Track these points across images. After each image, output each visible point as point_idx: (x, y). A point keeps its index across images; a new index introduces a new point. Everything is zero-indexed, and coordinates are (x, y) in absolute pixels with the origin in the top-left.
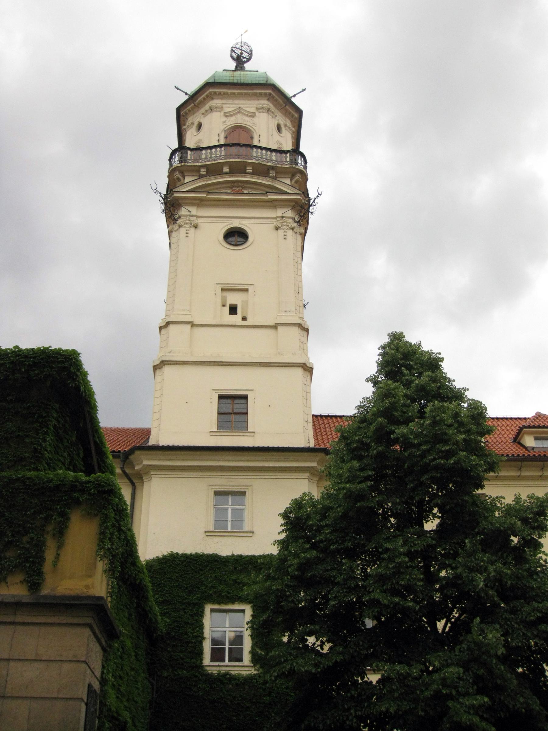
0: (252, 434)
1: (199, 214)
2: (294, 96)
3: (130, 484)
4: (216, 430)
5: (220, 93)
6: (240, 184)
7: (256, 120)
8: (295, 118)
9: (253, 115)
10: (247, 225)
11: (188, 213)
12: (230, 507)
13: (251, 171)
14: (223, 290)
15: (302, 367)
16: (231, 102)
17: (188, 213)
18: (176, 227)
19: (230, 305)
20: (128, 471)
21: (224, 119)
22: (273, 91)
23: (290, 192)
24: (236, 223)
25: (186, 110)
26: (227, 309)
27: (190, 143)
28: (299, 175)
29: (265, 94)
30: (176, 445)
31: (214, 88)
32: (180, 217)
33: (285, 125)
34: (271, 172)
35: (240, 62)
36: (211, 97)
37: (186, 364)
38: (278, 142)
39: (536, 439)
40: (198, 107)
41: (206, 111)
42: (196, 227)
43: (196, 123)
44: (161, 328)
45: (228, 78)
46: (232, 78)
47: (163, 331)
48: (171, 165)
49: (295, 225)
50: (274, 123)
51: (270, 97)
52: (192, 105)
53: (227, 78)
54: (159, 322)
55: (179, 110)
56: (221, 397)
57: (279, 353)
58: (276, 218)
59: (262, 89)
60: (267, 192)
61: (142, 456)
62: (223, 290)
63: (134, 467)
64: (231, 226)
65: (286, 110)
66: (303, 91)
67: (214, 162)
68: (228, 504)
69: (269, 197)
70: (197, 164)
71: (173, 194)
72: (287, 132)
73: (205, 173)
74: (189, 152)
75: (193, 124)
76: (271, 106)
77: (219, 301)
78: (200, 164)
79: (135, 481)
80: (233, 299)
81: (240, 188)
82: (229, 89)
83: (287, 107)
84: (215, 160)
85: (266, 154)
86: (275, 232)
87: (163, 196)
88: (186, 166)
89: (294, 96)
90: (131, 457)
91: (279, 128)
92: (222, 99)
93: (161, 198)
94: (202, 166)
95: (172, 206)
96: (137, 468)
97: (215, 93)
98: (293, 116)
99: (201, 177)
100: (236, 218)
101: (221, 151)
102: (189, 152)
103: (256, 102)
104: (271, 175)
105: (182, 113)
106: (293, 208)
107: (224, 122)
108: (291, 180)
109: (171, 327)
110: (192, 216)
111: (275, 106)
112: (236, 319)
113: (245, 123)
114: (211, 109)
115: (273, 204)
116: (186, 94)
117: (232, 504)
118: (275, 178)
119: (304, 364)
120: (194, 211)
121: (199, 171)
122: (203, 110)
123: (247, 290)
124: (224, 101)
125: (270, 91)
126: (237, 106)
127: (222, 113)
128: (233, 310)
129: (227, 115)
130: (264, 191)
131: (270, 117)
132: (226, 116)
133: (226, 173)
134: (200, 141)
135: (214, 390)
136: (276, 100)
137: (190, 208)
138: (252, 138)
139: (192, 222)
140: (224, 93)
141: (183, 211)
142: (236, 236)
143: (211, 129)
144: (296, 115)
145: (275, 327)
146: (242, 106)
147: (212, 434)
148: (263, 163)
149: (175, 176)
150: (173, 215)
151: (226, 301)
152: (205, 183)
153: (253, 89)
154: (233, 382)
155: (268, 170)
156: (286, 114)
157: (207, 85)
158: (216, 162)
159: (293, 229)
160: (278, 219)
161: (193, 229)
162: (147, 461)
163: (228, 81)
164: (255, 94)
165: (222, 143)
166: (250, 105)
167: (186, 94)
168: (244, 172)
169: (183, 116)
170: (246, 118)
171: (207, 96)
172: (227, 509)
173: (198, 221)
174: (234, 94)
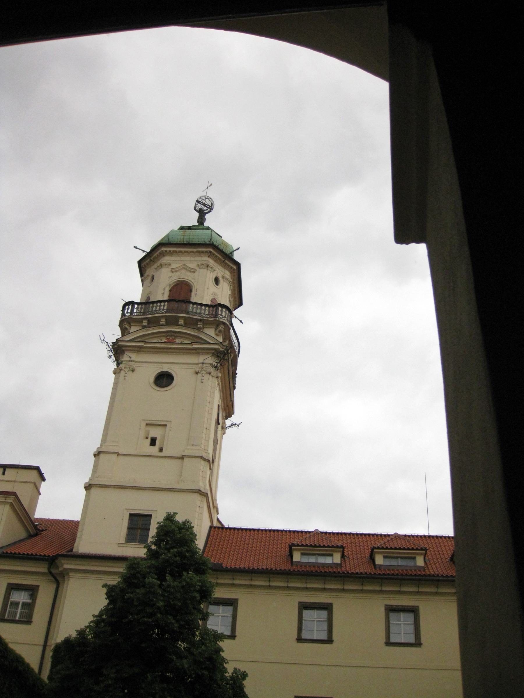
1: (136, 360)
4: (123, 542)
5: (170, 251)
6: (173, 334)
7: (196, 275)
8: (234, 269)
9: (193, 271)
10: (175, 370)
11: (128, 359)
14: (147, 425)
15: (198, 493)
16: (179, 259)
20: (53, 571)
21: (170, 274)
22: (214, 249)
23: (211, 342)
24: (166, 368)
26: (149, 441)
28: (222, 326)
29: (206, 252)
33: (223, 277)
34: (199, 323)
35: (202, 215)
36: (163, 254)
37: (109, 487)
38: (214, 294)
39: (385, 557)
40: (153, 261)
41: (158, 266)
42: (133, 371)
43: (151, 276)
45: (179, 237)
46: (182, 237)
48: (123, 314)
49: (212, 370)
50: (211, 276)
51: (210, 255)
55: (140, 263)
56: (131, 515)
58: (198, 364)
59: (204, 248)
61: (63, 561)
62: (147, 425)
65: (226, 263)
72: (225, 283)
73: (146, 324)
75: (148, 276)
76: (211, 262)
77: (142, 434)
79: (59, 579)
81: (173, 337)
83: (226, 261)
84: (155, 314)
85: (197, 308)
86: (195, 375)
88: (132, 318)
90: (56, 561)
91: (217, 281)
92: (172, 256)
93: (107, 347)
94: (144, 319)
96: (60, 569)
97: (166, 251)
98: (232, 268)
99: (144, 327)
103: (199, 259)
104: (198, 326)
105: (142, 265)
106: (213, 354)
107: (171, 277)
108: (216, 330)
110: (132, 361)
111: (215, 261)
112: (154, 450)
114: (161, 266)
115: (197, 352)
116: (144, 251)
118: (199, 329)
119: (199, 490)
120: (134, 356)
121: (142, 322)
122: (155, 266)
124: (173, 258)
125: (211, 250)
126: (183, 263)
127: (170, 270)
128: (153, 442)
129: (172, 271)
131: (209, 271)
132: (173, 272)
133: (163, 325)
135: (126, 509)
136: (216, 256)
137: (130, 354)
140: (174, 251)
142: (164, 379)
144: (235, 267)
145: (182, 458)
146: (185, 263)
147: (120, 545)
149: (125, 323)
151: (148, 434)
156: (226, 267)
157: (160, 245)
159: (210, 373)
161: (131, 372)
162: (67, 565)
164: (199, 252)
166: (192, 261)
170: (189, 274)
171: (160, 253)
173: (136, 366)
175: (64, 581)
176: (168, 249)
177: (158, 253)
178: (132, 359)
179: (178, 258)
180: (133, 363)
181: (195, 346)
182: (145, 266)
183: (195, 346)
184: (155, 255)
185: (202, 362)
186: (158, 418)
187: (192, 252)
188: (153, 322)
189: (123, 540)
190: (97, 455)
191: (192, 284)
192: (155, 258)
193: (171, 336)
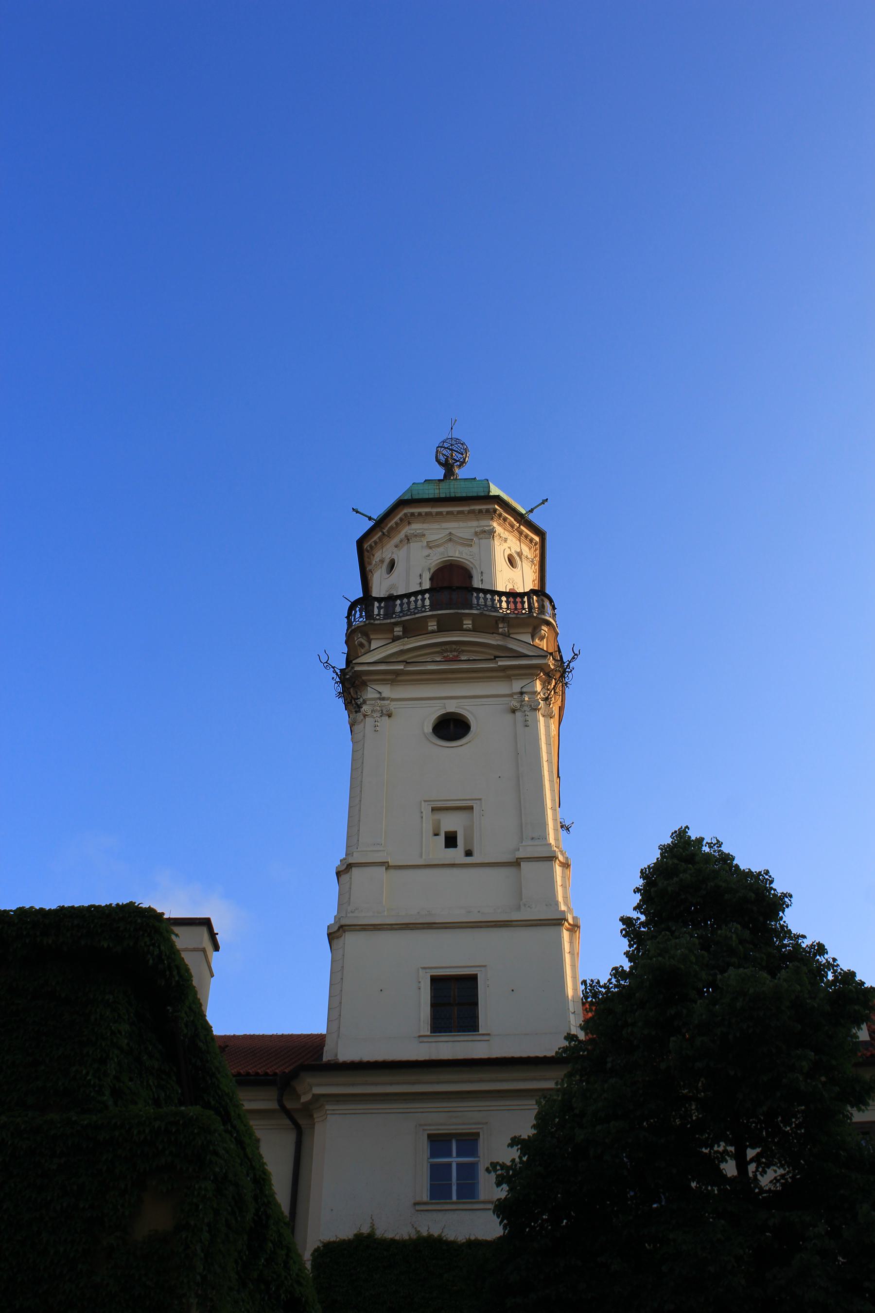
0: (486, 1038)
1: (393, 696)
2: (531, 511)
3: (293, 1126)
5: (420, 514)
6: (454, 647)
7: (474, 549)
9: (468, 543)
11: (378, 696)
12: (454, 1160)
13: (470, 626)
17: (378, 696)
18: (360, 716)
19: (446, 833)
20: (289, 1105)
21: (427, 552)
24: (452, 707)
25: (371, 542)
26: (442, 839)
27: (378, 591)
30: (366, 1058)
31: (411, 507)
32: (364, 702)
34: (501, 625)
36: (408, 520)
37: (379, 929)
40: (388, 535)
42: (390, 716)
43: (387, 561)
44: (339, 874)
46: (437, 491)
47: (345, 878)
48: (350, 624)
52: (380, 534)
53: (431, 492)
54: (335, 863)
55: (360, 543)
56: (434, 980)
57: (525, 905)
58: (511, 695)
60: (496, 657)
62: (433, 809)
63: (299, 1097)
64: (443, 712)
66: (543, 503)
67: (413, 617)
68: (449, 1155)
69: (500, 663)
70: (389, 621)
71: (353, 668)
74: (376, 604)
77: (428, 828)
78: (393, 620)
79: (300, 1122)
80: (450, 823)
81: (455, 654)
82: (432, 507)
84: (415, 614)
87: (338, 671)
88: (372, 624)
89: (531, 511)
92: (423, 523)
93: (335, 676)
94: (396, 624)
95: (352, 685)
97: (412, 514)
98: (531, 540)
99: (395, 639)
100: (453, 698)
101: (423, 600)
102: (376, 604)
104: (500, 630)
107: (428, 556)
109: (355, 871)
110: (383, 699)
112: (456, 855)
113: (457, 555)
114: (408, 539)
116: (370, 519)
117: (458, 1155)
118: (507, 635)
120: (386, 691)
122: (396, 540)
123: (471, 808)
124: (425, 526)
126: (447, 532)
128: (451, 840)
130: (491, 654)
132: (431, 548)
133: (433, 632)
134: (393, 586)
137: (379, 688)
138: (470, 577)
139: (384, 708)
140: (427, 514)
141: (370, 693)
142: (451, 728)
143: (410, 568)
144: (537, 539)
145: (516, 863)
147: (422, 1039)
148: (487, 613)
149: (356, 640)
150: (355, 699)
152: (402, 648)
153: (469, 505)
154: (453, 955)
155: (497, 623)
157: (401, 503)
158: (417, 616)
160: (515, 697)
163: (431, 496)
165: (428, 587)
167: (370, 519)
168: (460, 628)
169: (368, 551)
171: (401, 519)
172: (449, 1165)
173: (393, 706)
174: (439, 514)
175: (312, 1127)
176: (416, 510)
177: (397, 519)
178: (384, 695)
179: (436, 526)
180: (386, 702)
181: (502, 663)
182: (371, 546)
183: (502, 663)
184: (392, 523)
185: (519, 690)
186: (455, 794)
187: (462, 512)
188: (412, 629)
189: (426, 1030)
190: (344, 871)
191: (471, 565)
192: (392, 528)
193: (451, 652)
